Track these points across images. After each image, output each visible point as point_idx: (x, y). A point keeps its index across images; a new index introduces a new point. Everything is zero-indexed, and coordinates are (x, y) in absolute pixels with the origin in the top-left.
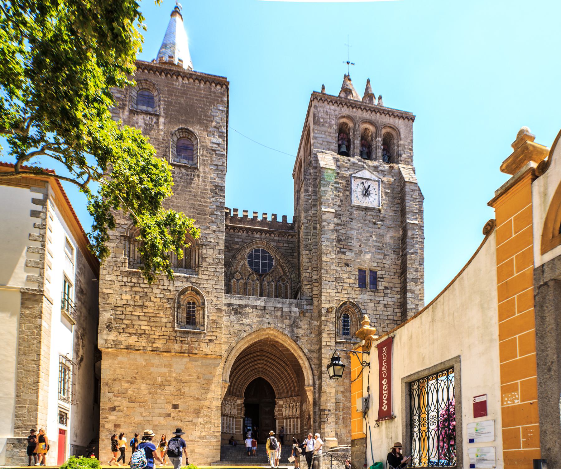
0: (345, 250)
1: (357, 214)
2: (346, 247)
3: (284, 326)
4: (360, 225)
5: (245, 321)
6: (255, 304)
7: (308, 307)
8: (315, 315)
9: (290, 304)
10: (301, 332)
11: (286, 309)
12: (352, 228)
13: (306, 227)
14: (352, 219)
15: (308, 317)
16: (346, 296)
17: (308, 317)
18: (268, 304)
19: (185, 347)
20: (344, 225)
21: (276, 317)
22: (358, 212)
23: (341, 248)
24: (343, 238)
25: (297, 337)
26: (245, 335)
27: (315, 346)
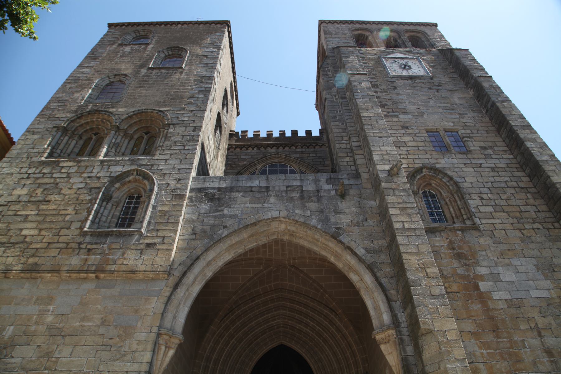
0: (396, 114)
1: (399, 83)
2: (398, 110)
3: (309, 212)
4: (409, 91)
5: (226, 211)
6: (249, 184)
7: (352, 182)
8: (368, 191)
9: (316, 181)
10: (344, 220)
11: (309, 187)
12: (398, 94)
13: (331, 101)
14: (394, 87)
15: (354, 196)
16: (416, 161)
17: (354, 196)
18: (272, 183)
19: (94, 259)
20: (386, 92)
21: (291, 200)
22: (401, 81)
23: (389, 112)
24: (389, 103)
25: (338, 229)
26: (225, 234)
27: (380, 242)
